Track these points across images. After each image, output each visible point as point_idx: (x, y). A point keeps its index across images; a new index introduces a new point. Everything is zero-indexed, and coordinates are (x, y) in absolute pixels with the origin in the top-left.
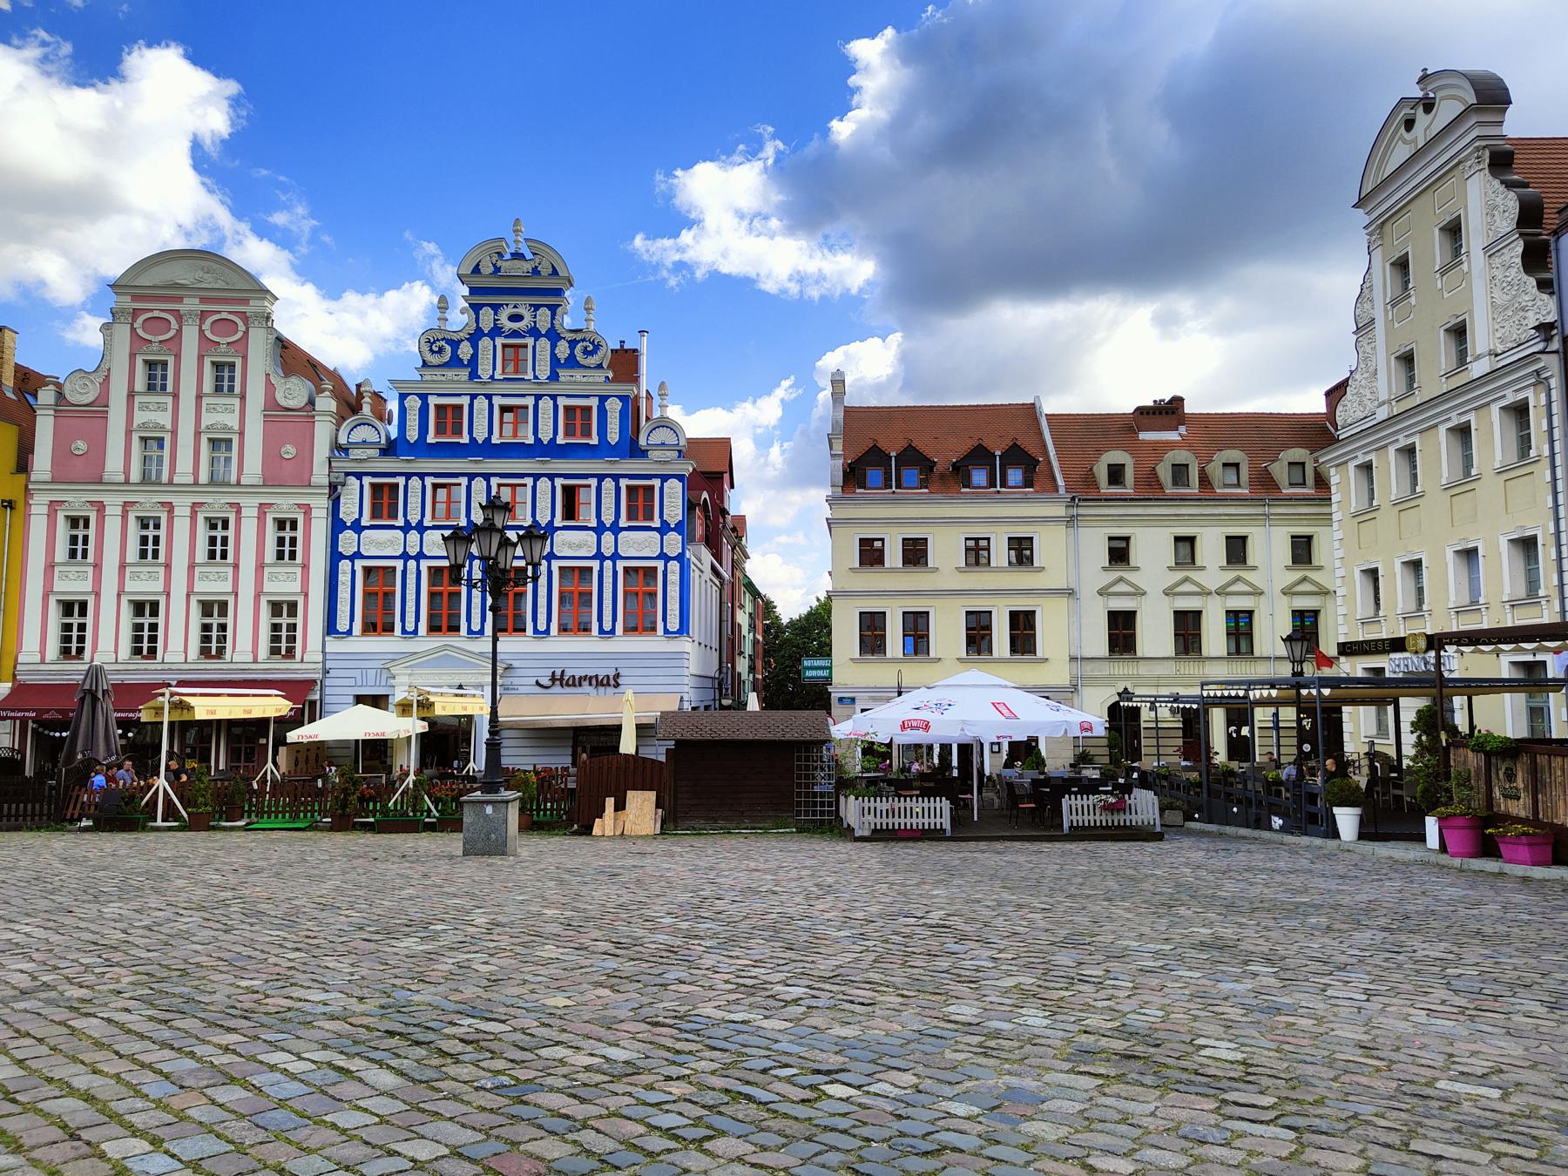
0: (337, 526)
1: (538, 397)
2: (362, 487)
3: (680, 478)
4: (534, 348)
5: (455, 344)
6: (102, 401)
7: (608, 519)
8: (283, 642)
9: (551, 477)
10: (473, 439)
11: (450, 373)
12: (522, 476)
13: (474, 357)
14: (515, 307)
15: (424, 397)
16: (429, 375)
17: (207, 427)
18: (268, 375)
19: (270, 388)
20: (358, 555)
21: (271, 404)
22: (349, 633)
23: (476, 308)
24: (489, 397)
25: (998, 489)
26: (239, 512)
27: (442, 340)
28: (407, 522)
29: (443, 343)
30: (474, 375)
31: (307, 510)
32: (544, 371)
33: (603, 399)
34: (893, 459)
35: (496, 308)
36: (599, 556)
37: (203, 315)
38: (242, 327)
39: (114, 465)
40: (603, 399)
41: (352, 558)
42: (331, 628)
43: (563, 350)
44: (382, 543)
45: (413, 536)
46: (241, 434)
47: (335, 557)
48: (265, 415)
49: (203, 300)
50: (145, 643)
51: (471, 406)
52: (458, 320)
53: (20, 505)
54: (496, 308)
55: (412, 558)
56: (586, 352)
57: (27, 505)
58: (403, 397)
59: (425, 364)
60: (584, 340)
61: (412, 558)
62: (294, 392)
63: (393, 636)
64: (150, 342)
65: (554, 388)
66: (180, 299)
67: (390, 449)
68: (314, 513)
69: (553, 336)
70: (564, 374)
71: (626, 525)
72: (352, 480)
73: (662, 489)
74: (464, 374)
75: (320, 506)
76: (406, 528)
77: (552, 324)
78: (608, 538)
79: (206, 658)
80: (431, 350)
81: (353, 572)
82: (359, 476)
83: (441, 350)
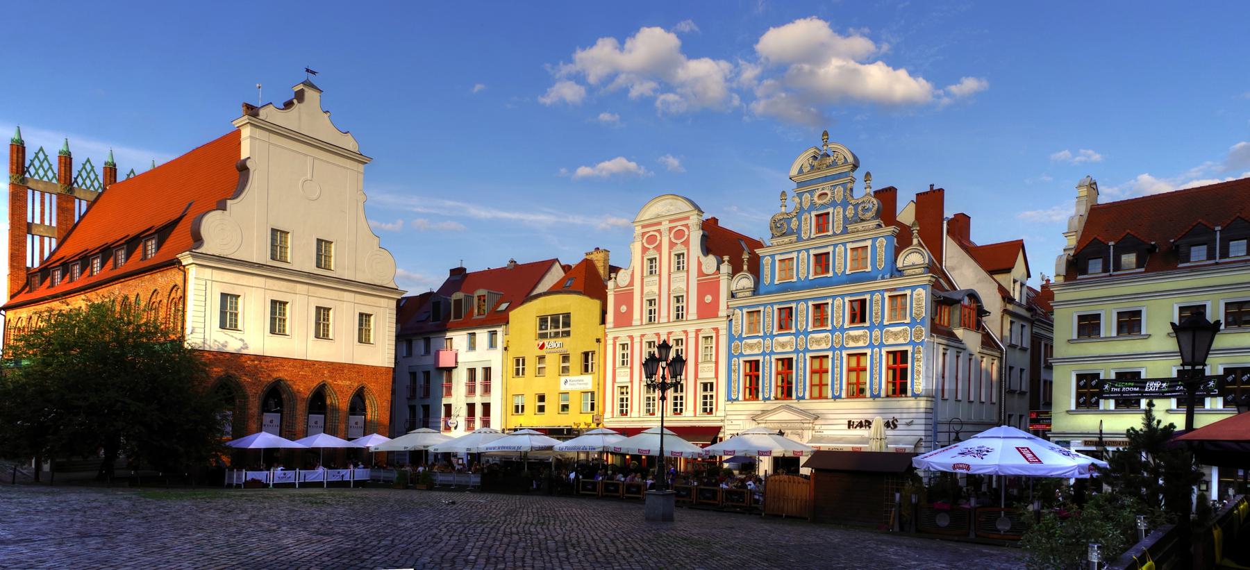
0: (731, 338)
2: (742, 314)
3: (923, 287)
4: (833, 213)
6: (631, 283)
7: (877, 321)
9: (842, 296)
10: (799, 278)
11: (786, 239)
12: (826, 298)
13: (800, 225)
15: (772, 256)
17: (673, 291)
18: (699, 257)
19: (700, 264)
20: (741, 355)
21: (700, 273)
24: (807, 250)
25: (1218, 260)
26: (687, 336)
31: (716, 330)
34: (1112, 247)
36: (871, 346)
37: (671, 229)
38: (687, 233)
39: (636, 315)
41: (738, 357)
42: (730, 399)
45: (768, 341)
46: (687, 292)
47: (730, 356)
48: (698, 280)
49: (671, 221)
51: (798, 257)
53: (602, 341)
55: (767, 354)
57: (606, 341)
61: (767, 354)
62: (710, 262)
64: (649, 249)
66: (660, 224)
68: (720, 333)
71: (888, 323)
72: (737, 311)
73: (911, 296)
74: (794, 238)
75: (723, 325)
76: (763, 337)
78: (877, 332)
82: (741, 308)
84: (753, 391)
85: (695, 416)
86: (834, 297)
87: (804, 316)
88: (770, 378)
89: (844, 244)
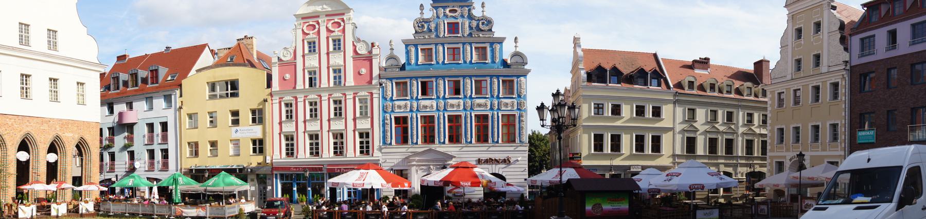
1: (464, 44)
5: (427, 21)
8: (365, 148)
14: (453, 7)
16: (416, 35)
22: (391, 144)
23: (436, 8)
27: (423, 22)
28: (412, 98)
29: (423, 23)
30: (437, 36)
32: (467, 31)
33: (492, 44)
35: (444, 8)
40: (492, 44)
43: (474, 23)
44: (402, 107)
50: (315, 150)
52: (428, 14)
54: (444, 8)
56: (483, 24)
58: (407, 46)
59: (416, 32)
60: (482, 19)
63: (408, 145)
65: (471, 40)
67: (403, 68)
69: (471, 17)
70: (475, 34)
77: (469, 14)
79: (336, 155)
80: (418, 26)
81: (391, 119)
83: (423, 26)
84: (404, 139)
85: (355, 157)
86: (464, 77)
87: (443, 87)
88: (416, 130)
89: (470, 44)
